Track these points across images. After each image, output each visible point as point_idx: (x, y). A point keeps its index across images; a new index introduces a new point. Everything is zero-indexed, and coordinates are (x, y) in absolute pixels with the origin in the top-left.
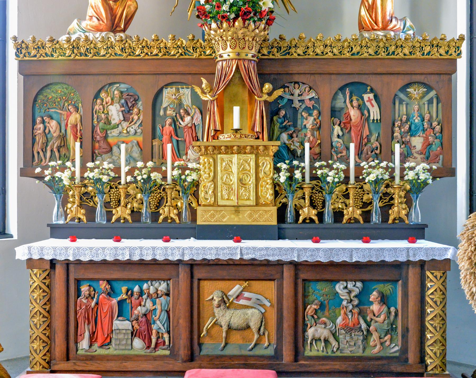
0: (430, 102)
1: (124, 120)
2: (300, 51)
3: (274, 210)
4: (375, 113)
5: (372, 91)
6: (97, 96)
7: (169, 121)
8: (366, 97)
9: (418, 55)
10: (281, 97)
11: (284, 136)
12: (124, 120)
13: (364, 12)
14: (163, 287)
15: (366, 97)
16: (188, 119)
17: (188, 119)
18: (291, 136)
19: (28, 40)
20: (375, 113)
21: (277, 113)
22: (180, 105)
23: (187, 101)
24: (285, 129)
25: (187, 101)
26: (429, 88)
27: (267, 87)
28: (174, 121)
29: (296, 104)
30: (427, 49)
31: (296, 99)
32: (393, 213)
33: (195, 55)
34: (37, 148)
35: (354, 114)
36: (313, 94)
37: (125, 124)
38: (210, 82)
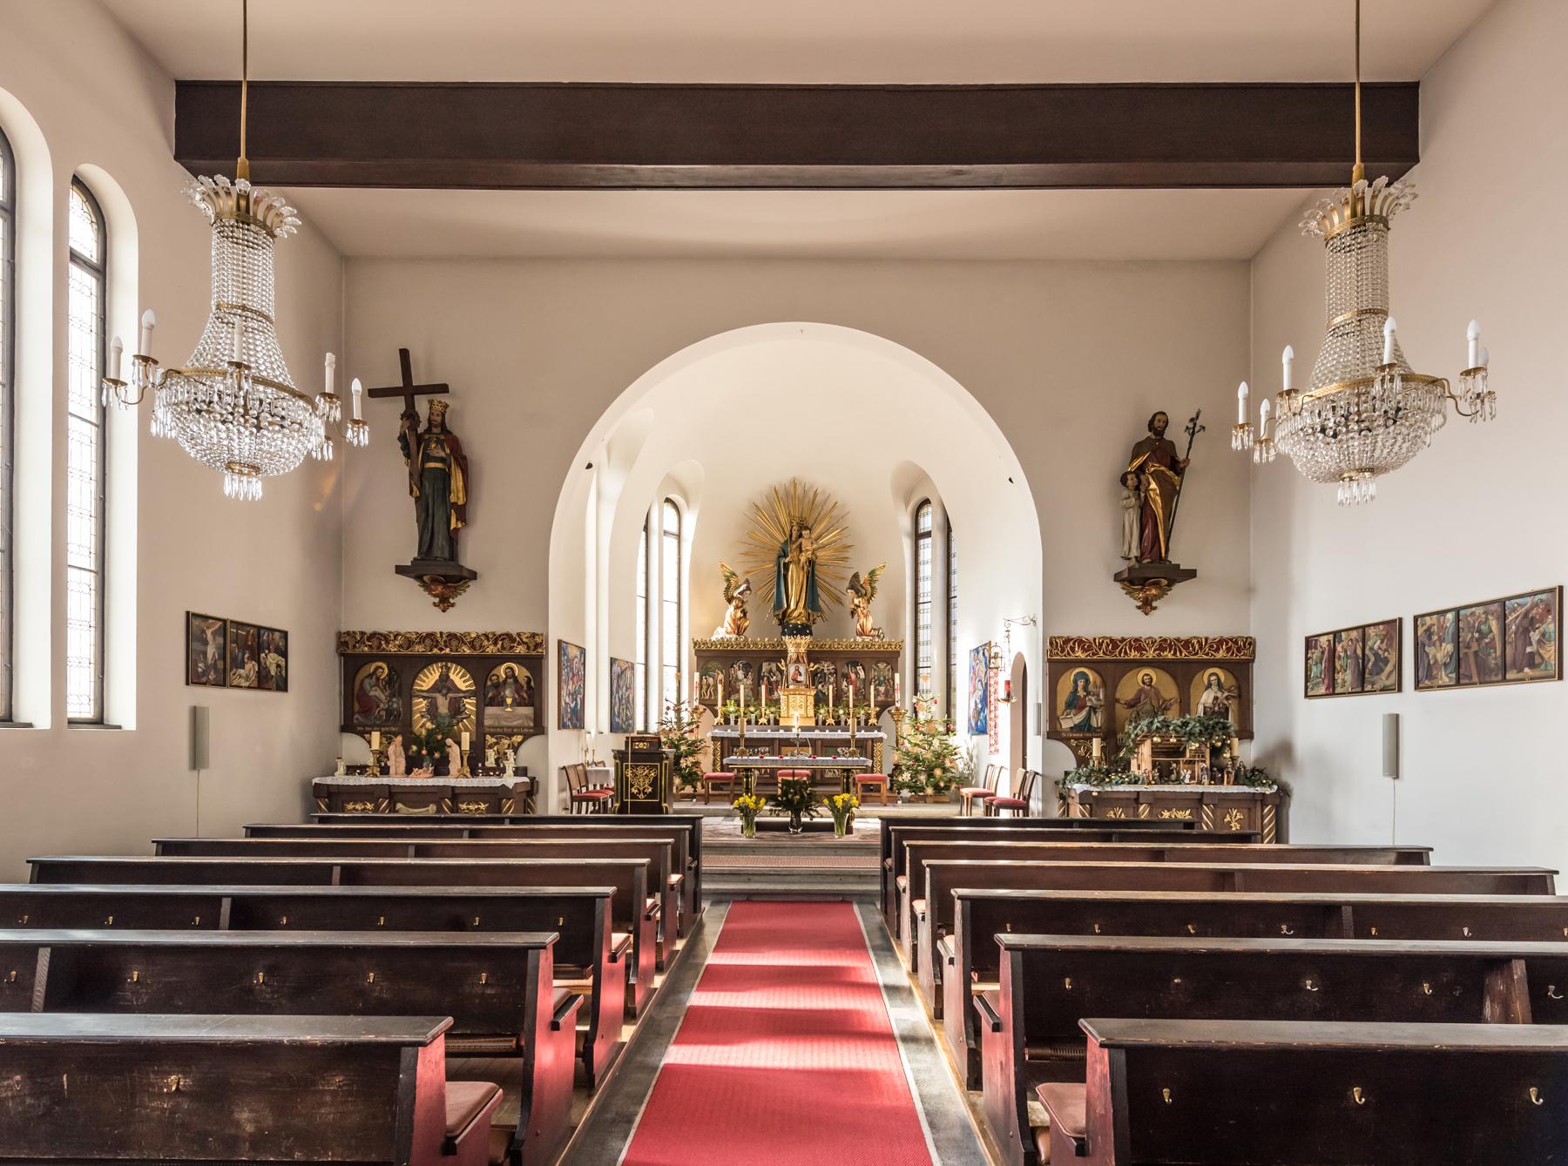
0: (889, 670)
1: (745, 677)
2: (827, 646)
3: (814, 720)
4: (862, 675)
5: (861, 665)
6: (732, 666)
7: (766, 678)
8: (858, 668)
9: (882, 649)
10: (818, 668)
11: (820, 686)
12: (745, 677)
13: (858, 626)
14: (767, 749)
15: (858, 668)
16: (775, 677)
17: (775, 677)
18: (823, 686)
19: (699, 640)
20: (862, 675)
21: (816, 675)
22: (770, 671)
23: (774, 669)
24: (820, 683)
25: (774, 669)
26: (888, 664)
27: (812, 664)
28: (768, 678)
29: (826, 671)
30: (886, 646)
31: (826, 669)
32: (871, 721)
33: (778, 648)
34: (704, 691)
35: (853, 676)
36: (833, 667)
37: (745, 680)
38: (785, 661)
